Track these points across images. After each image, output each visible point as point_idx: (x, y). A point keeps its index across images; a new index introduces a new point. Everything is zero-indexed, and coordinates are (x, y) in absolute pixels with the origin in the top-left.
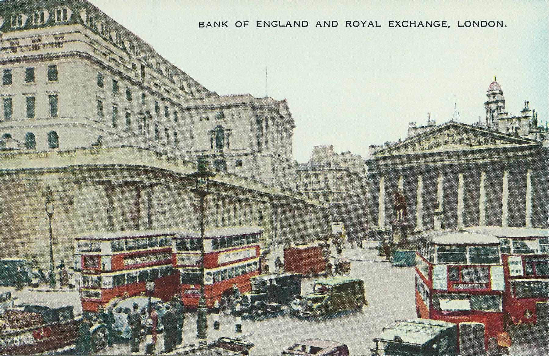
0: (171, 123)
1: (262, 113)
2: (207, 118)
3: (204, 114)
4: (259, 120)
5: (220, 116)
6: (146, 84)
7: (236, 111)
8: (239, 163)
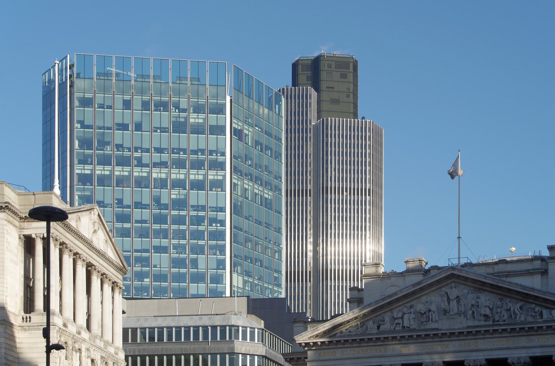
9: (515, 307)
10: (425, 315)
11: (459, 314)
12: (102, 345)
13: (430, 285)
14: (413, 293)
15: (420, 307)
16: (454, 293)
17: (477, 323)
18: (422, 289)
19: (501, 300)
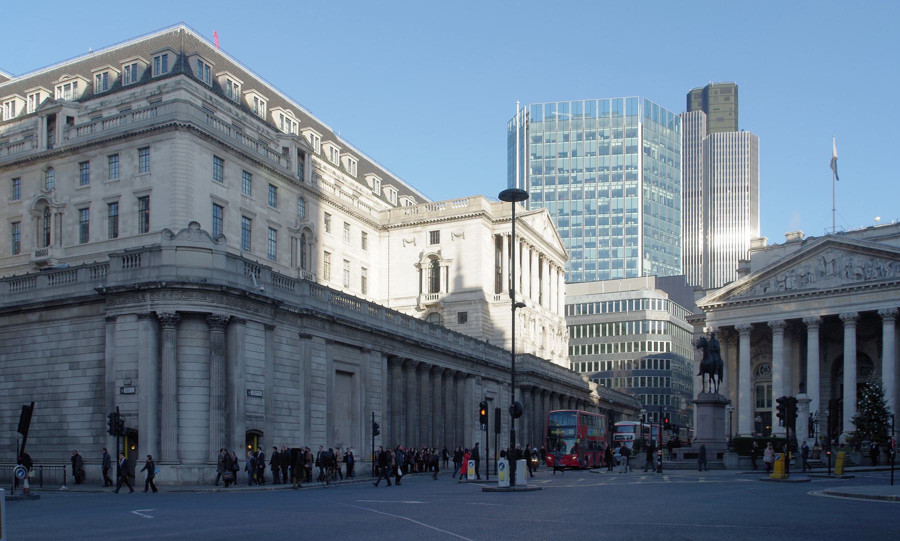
2: (414, 242)
3: (407, 233)
5: (435, 237)
9: (884, 265)
10: (805, 277)
11: (834, 274)
13: (809, 252)
14: (794, 260)
15: (801, 271)
16: (830, 257)
17: (851, 281)
18: (802, 256)
19: (872, 260)
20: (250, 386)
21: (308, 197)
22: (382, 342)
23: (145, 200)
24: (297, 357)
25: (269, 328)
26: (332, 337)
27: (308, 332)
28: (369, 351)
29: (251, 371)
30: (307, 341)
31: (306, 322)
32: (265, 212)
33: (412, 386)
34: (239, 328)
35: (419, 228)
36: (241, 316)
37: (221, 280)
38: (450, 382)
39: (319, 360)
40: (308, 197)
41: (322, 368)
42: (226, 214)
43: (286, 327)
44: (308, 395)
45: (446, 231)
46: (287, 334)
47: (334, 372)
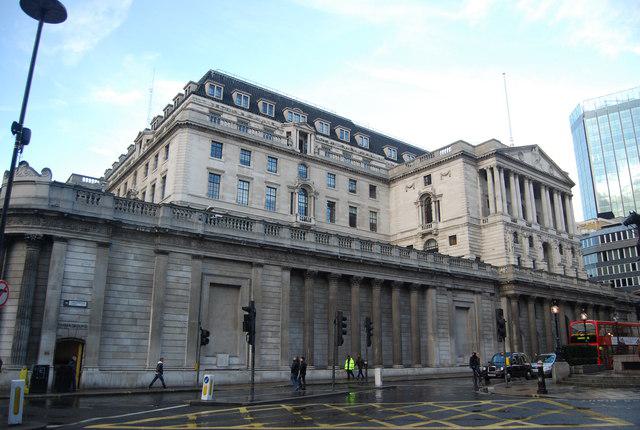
0: (362, 199)
1: (486, 164)
3: (409, 181)
4: (483, 174)
6: (311, 152)
7: (444, 169)
8: (453, 240)
12: (554, 233)
20: (67, 297)
21: (309, 163)
22: (281, 257)
23: (164, 178)
24: (149, 271)
25: (101, 245)
26: (201, 253)
27: (161, 248)
28: (260, 265)
29: (73, 283)
30: (162, 258)
31: (158, 240)
32: (264, 176)
33: (131, 283)
34: (57, 246)
35: (416, 176)
36: (59, 234)
37: (43, 205)
38: (414, 295)
39: (181, 274)
40: (309, 163)
41: (185, 281)
42: (222, 180)
43: (134, 245)
44: (162, 307)
45: (435, 174)
46: (138, 251)
47: (206, 288)
